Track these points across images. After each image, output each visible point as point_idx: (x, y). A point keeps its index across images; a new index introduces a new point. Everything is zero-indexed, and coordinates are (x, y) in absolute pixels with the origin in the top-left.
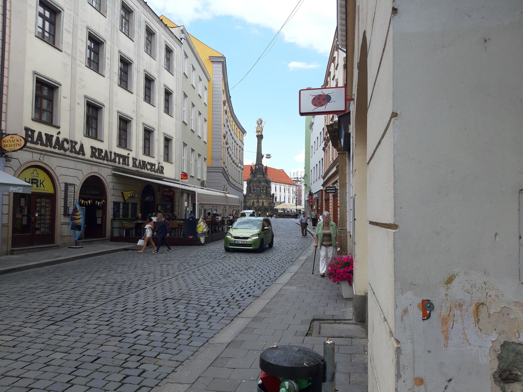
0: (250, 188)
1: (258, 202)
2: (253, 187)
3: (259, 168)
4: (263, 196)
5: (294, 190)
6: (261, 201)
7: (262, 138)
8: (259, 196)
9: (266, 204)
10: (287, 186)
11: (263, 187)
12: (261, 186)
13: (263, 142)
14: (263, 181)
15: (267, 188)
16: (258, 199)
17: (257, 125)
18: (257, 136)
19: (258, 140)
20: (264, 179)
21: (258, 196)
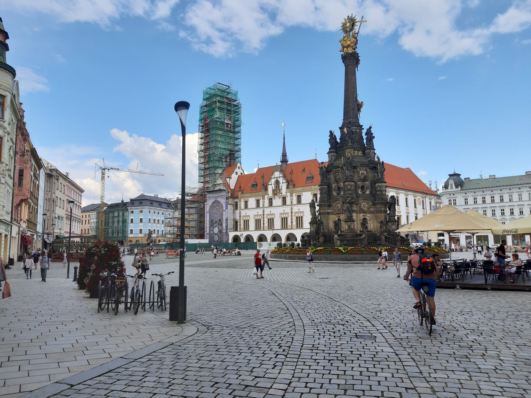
0: (329, 186)
1: (350, 220)
2: (337, 181)
3: (351, 133)
4: (364, 205)
5: (433, 204)
6: (358, 217)
8: (351, 203)
9: (372, 225)
10: (419, 197)
11: (365, 179)
12: (356, 178)
13: (360, 73)
14: (363, 165)
16: (351, 212)
18: (345, 58)
20: (365, 160)
21: (351, 203)
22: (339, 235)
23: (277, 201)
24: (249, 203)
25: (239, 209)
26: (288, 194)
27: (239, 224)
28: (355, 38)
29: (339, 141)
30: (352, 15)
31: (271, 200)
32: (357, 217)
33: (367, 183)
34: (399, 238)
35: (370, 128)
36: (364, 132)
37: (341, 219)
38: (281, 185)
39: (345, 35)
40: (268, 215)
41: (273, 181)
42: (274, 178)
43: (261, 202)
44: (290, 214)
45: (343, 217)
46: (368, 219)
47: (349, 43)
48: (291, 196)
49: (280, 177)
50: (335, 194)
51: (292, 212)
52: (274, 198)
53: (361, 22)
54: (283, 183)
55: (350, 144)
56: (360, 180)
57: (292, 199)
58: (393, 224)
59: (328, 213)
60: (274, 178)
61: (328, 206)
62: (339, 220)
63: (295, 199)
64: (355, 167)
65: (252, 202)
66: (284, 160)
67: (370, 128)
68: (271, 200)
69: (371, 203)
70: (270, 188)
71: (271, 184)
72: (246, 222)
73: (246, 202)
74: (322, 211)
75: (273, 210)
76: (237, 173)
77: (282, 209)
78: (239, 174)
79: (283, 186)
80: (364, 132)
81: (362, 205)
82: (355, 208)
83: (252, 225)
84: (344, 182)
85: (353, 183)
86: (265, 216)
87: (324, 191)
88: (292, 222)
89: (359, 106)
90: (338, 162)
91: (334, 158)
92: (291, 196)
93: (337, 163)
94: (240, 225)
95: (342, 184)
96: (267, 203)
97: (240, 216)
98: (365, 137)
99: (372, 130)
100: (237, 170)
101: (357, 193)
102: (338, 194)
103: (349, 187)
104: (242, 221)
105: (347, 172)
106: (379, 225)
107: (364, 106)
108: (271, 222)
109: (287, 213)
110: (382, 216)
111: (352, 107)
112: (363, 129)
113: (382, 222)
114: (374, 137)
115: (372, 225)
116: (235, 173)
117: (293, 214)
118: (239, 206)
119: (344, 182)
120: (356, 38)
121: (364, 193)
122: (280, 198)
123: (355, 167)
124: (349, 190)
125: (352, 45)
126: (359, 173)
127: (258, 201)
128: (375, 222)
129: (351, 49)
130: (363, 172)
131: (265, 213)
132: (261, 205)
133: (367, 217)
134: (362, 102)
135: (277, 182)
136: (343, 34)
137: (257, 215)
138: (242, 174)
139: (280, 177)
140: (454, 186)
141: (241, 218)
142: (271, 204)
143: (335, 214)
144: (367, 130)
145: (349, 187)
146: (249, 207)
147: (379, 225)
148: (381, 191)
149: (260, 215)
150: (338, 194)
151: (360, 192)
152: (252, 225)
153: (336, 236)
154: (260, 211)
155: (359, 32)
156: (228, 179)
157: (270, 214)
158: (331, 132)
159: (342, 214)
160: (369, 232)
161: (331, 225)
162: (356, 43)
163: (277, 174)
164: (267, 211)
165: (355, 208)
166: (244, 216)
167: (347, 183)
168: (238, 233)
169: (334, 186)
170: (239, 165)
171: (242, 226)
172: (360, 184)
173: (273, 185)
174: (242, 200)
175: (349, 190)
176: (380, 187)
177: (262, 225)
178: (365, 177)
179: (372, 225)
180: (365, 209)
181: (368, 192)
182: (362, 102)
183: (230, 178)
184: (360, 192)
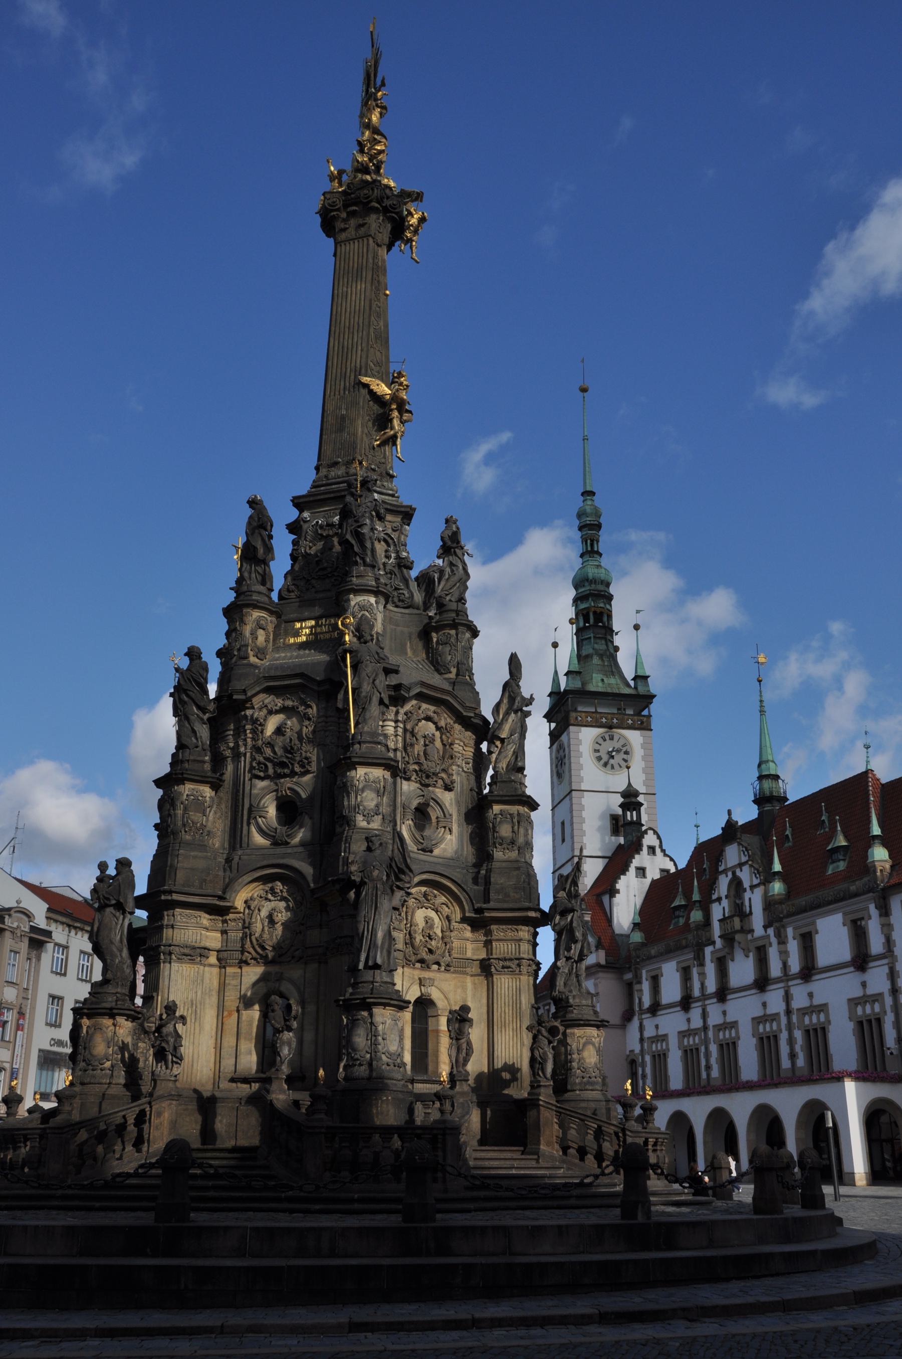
23: (742, 970)
25: (637, 1008)
26: (771, 931)
38: (747, 895)
43: (695, 971)
44: (784, 1020)
48: (782, 941)
49: (741, 865)
51: (788, 1012)
52: (731, 953)
54: (752, 887)
57: (784, 954)
60: (725, 871)
63: (793, 946)
70: (717, 912)
76: (641, 872)
78: (653, 874)
86: (710, 1034)
88: (793, 1056)
97: (642, 1040)
100: (641, 859)
104: (648, 1058)
116: (632, 870)
118: (637, 1001)
135: (736, 885)
139: (741, 865)
163: (732, 854)
170: (649, 839)
173: (725, 903)
177: (704, 1075)
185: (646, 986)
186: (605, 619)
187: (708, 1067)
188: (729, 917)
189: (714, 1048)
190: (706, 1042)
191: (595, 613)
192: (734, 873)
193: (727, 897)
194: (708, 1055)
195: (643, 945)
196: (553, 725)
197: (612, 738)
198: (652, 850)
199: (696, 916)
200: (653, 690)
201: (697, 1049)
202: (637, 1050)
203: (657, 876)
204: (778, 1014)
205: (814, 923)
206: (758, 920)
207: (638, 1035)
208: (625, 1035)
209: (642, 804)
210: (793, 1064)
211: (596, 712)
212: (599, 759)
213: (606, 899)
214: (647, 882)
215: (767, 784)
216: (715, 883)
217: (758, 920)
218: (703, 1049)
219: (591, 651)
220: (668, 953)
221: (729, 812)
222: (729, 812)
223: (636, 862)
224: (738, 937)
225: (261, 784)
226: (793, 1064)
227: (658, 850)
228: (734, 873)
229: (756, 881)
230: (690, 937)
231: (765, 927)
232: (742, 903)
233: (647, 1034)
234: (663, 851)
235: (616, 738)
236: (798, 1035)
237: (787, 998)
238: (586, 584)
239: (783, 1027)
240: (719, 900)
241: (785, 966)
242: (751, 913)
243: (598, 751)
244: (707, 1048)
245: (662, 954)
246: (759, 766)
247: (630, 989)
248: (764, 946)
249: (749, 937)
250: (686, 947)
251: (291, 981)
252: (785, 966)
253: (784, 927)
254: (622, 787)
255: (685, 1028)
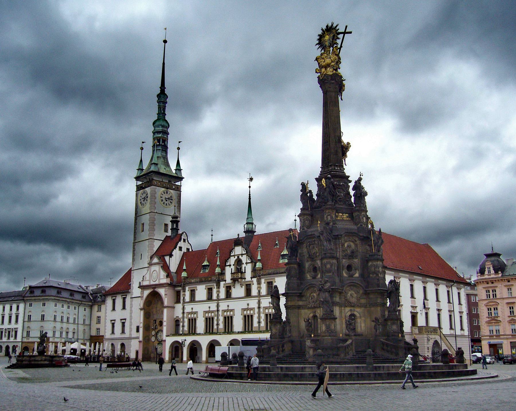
0: (300, 266)
1: (330, 317)
2: (312, 258)
4: (352, 295)
7: (341, 87)
8: (332, 292)
9: (363, 325)
11: (352, 255)
12: (339, 254)
15: (365, 261)
17: (318, 52)
18: (322, 82)
19: (325, 93)
22: (313, 341)
23: (238, 291)
24: (197, 292)
25: (182, 302)
26: (255, 280)
27: (181, 324)
28: (336, 55)
29: (315, 197)
30: (332, 25)
31: (228, 289)
32: (341, 312)
33: (356, 260)
34: (402, 344)
35: (360, 179)
36: (351, 185)
37: (318, 315)
38: (243, 266)
39: (323, 51)
40: (224, 311)
41: (232, 260)
42: (234, 256)
43: (215, 291)
44: (256, 310)
45: (319, 312)
46: (357, 315)
47: (328, 61)
48: (259, 283)
49: (242, 255)
50: (308, 277)
51: (259, 308)
53: (345, 33)
54: (247, 263)
55: (330, 203)
56: (345, 256)
58: (393, 324)
59: (299, 307)
60: (234, 256)
61: (298, 296)
62: (315, 317)
64: (337, 237)
65: (201, 292)
66: (250, 232)
67: (360, 179)
68: (228, 289)
69: (361, 292)
70: (228, 271)
71: (230, 265)
72: (192, 322)
73: (193, 293)
74: (290, 304)
75: (232, 304)
76: (180, 248)
77: (243, 304)
78: (184, 250)
79: (248, 269)
80: (351, 185)
81: (349, 295)
82: (337, 299)
83: (201, 326)
84: (322, 259)
85: (335, 261)
86: (220, 313)
87: (293, 272)
88: (259, 322)
89: (344, 149)
90: (312, 230)
91: (307, 223)
92: (259, 283)
93: (310, 231)
94: (183, 326)
95: (319, 262)
96: (223, 295)
97: (183, 313)
98: (352, 193)
99: (363, 183)
101: (340, 275)
102: (314, 278)
103: (328, 266)
104: (186, 320)
105: (325, 243)
106: (373, 324)
107: (350, 149)
108: (229, 321)
109: (252, 309)
110: (377, 312)
111: (334, 150)
112: (350, 182)
113: (376, 320)
114: (366, 194)
115: (363, 325)
117: (261, 310)
118: (182, 298)
119: (322, 259)
120: (338, 55)
121: (351, 276)
122: (241, 285)
123: (337, 237)
124: (329, 271)
125: (333, 64)
126: (343, 245)
127: (210, 290)
128: (368, 321)
129: (332, 70)
130: (349, 244)
131: (221, 309)
132: (215, 297)
133: (356, 313)
134: (348, 144)
135: (239, 262)
136: (320, 49)
137: (209, 312)
138: (188, 249)
139: (242, 255)
140: (492, 271)
141: (185, 315)
142: (228, 296)
143: (309, 308)
144: (356, 182)
145: (328, 266)
146: (197, 299)
147: (373, 324)
148: (376, 273)
149: (212, 312)
150: (314, 278)
151: (345, 275)
152: (201, 326)
153: (308, 343)
154: (213, 306)
155: (341, 46)
156: (167, 258)
157: (227, 311)
158: (303, 185)
159: (320, 307)
160: (359, 335)
161: (303, 325)
162: (338, 62)
164: (223, 306)
165: (337, 299)
166: (189, 313)
167: (325, 261)
168: (179, 339)
169: (307, 265)
171: (186, 328)
172: (345, 262)
174: (187, 288)
175: (329, 271)
176: (377, 266)
178: (353, 252)
179: (363, 325)
180: (353, 300)
181: (357, 275)
182: (348, 144)
183: (171, 256)
184: (345, 275)
185: (188, 294)
186: (166, 143)
187: (218, 325)
188: (234, 273)
189: (221, 319)
190: (218, 316)
191: (163, 139)
192: (238, 257)
193: (233, 265)
194: (218, 320)
195: (187, 277)
196: (140, 183)
197: (167, 193)
198: (184, 240)
199: (218, 270)
200: (183, 176)
201: (213, 318)
202: (181, 316)
203: (185, 251)
204: (254, 308)
205: (274, 279)
206: (248, 275)
207: (182, 311)
208: (174, 311)
209: (179, 221)
210: (259, 325)
211: (162, 181)
212: (162, 200)
213: (167, 258)
214: (183, 252)
215: (250, 226)
216: (228, 259)
217: (248, 275)
218: (216, 318)
219: (160, 155)
220: (201, 282)
221: (238, 235)
222: (238, 235)
223: (179, 245)
224: (239, 280)
225: (344, 260)
226: (259, 325)
227: (186, 241)
228: (238, 257)
229: (248, 261)
230: (214, 278)
231: (251, 278)
232: (241, 268)
233: (186, 311)
234: (188, 241)
235: (168, 193)
236: (263, 316)
237: (259, 303)
238: (160, 126)
239: (256, 312)
240: (230, 265)
241: (259, 291)
242: (245, 272)
243: (161, 197)
244: (218, 318)
245: (197, 282)
246: (247, 219)
247: (178, 294)
248: (250, 284)
249: (243, 280)
250: (211, 281)
251: (357, 312)
252: (259, 291)
253: (260, 279)
254: (172, 214)
255: (208, 310)
